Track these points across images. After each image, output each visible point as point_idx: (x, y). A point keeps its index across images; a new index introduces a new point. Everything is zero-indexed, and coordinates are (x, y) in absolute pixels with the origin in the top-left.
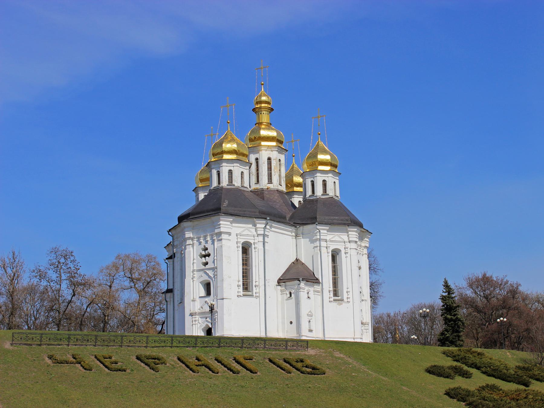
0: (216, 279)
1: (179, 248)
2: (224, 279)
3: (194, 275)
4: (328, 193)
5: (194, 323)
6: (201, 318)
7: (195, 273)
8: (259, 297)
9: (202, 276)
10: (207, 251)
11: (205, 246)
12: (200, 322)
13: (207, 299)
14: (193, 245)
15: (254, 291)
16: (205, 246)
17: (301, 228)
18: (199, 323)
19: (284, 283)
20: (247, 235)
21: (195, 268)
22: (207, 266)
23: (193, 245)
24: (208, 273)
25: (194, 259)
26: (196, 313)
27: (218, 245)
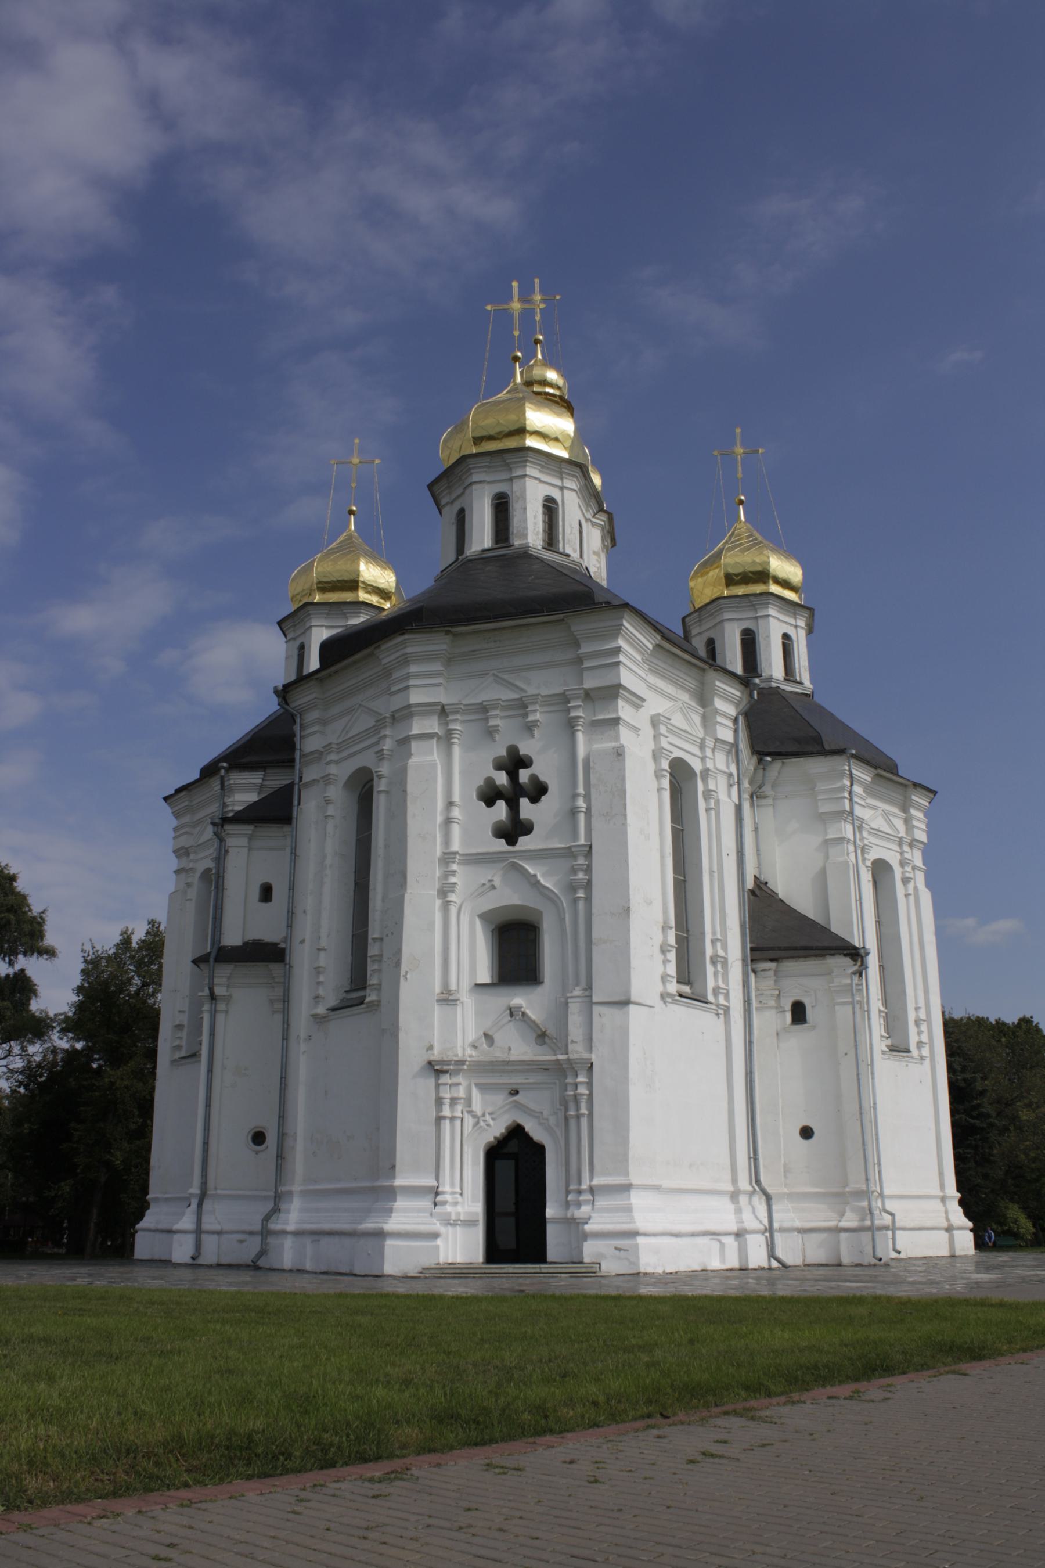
0: (581, 905)
1: (337, 762)
2: (632, 909)
3: (453, 880)
4: (798, 679)
5: (446, 1112)
6: (481, 1087)
7: (454, 867)
8: (727, 1010)
9: (493, 887)
10: (524, 776)
11: (513, 751)
12: (477, 1106)
13: (520, 998)
14: (449, 735)
15: (711, 983)
16: (513, 751)
17: (778, 765)
18: (469, 1112)
19: (772, 965)
20: (685, 731)
21: (456, 846)
22: (525, 843)
23: (446, 739)
24: (532, 872)
25: (450, 804)
26: (462, 1062)
27: (597, 746)
